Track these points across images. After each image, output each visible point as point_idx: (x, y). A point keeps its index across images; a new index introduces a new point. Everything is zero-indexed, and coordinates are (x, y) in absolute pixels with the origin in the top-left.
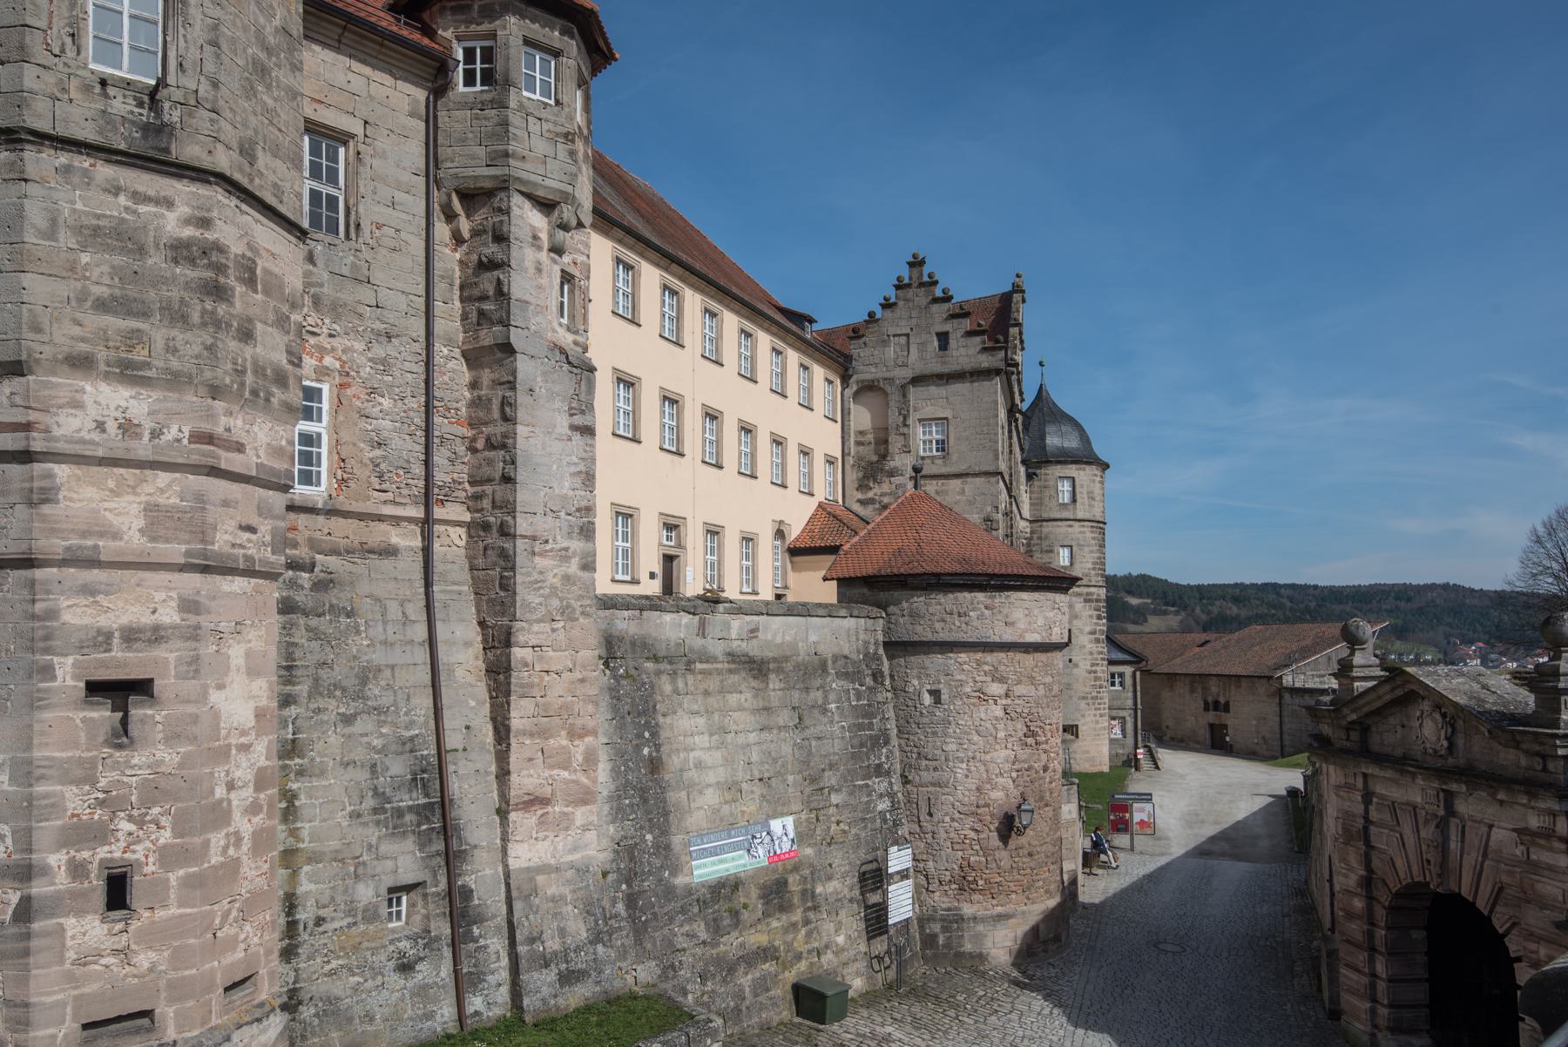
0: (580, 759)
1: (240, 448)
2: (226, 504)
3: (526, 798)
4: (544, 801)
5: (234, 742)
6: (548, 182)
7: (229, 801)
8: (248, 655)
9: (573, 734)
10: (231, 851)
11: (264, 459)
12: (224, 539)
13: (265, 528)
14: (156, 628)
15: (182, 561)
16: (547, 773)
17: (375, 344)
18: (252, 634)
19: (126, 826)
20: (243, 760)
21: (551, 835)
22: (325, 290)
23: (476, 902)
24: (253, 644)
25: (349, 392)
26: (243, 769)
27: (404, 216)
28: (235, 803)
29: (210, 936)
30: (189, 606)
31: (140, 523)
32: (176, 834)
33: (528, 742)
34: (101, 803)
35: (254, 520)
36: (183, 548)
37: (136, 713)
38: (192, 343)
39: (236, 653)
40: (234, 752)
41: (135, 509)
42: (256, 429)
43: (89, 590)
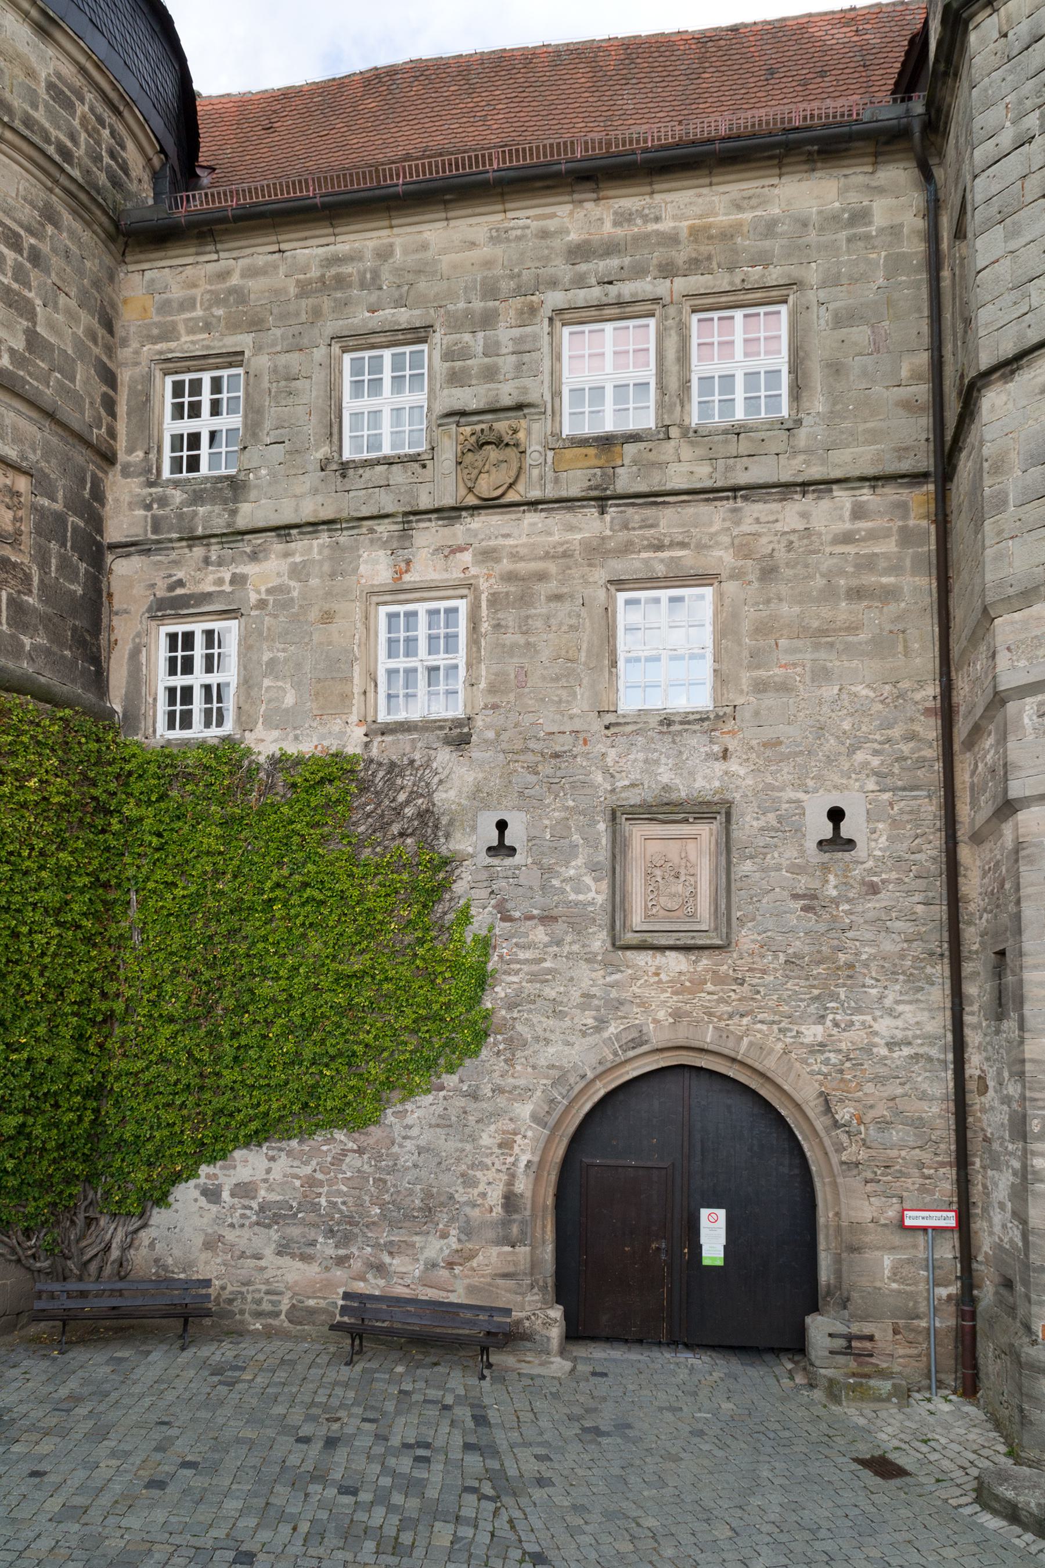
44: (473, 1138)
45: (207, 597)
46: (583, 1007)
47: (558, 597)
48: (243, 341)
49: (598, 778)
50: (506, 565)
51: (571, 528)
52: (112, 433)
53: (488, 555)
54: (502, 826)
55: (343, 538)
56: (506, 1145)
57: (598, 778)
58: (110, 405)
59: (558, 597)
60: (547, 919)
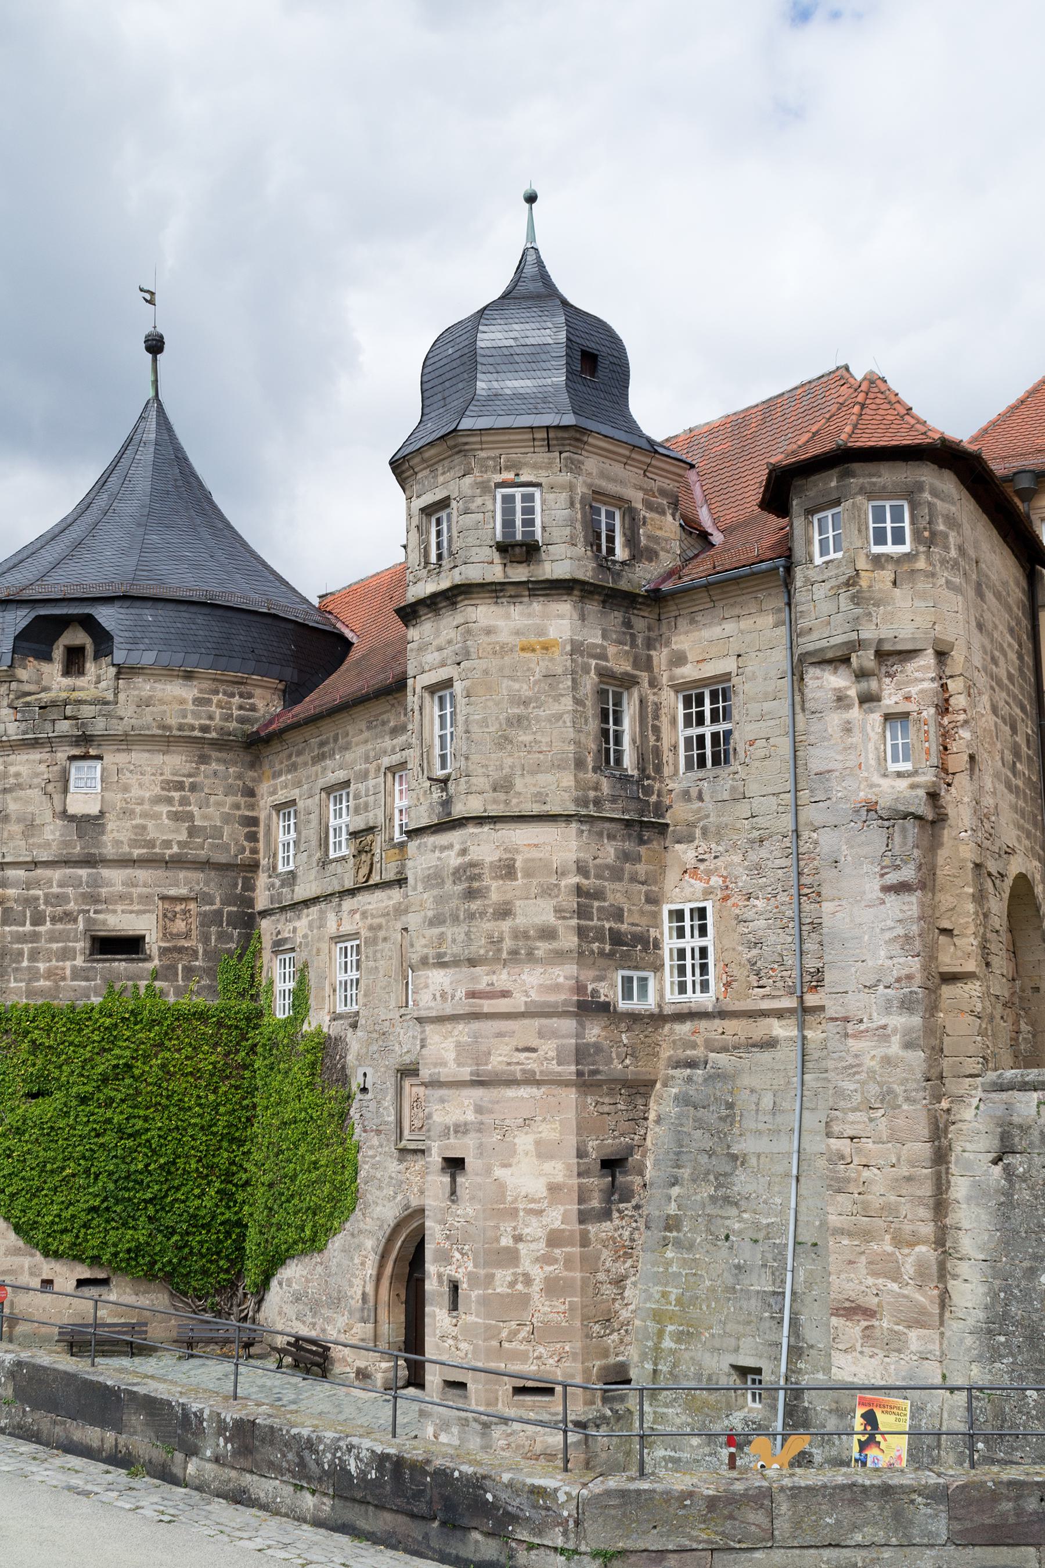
0: (911, 1271)
1: (505, 994)
2: (500, 1035)
3: (847, 1304)
4: (869, 1313)
5: (521, 1206)
6: (833, 641)
7: (517, 1251)
8: (538, 1143)
9: (898, 1241)
10: (519, 1287)
11: (534, 996)
12: (498, 1061)
13: (548, 1048)
14: (466, 1124)
15: (468, 1078)
16: (870, 1281)
17: (750, 852)
18: (544, 1127)
19: (458, 1255)
20: (534, 1220)
21: (881, 1355)
22: (711, 819)
23: (806, 1404)
24: (543, 1135)
25: (730, 903)
26: (534, 1228)
27: (772, 723)
28: (523, 1252)
29: (495, 1343)
30: (479, 1110)
31: (453, 1055)
32: (475, 1266)
33: (846, 1242)
34: (448, 1237)
35: (534, 1043)
36: (469, 1069)
37: (460, 1180)
38: (455, 932)
39: (524, 1141)
40: (521, 1214)
41: (452, 1045)
42: (523, 977)
43: (442, 1100)
44: (352, 1259)
45: (285, 940)
46: (389, 1185)
47: (385, 939)
48: (295, 793)
49: (397, 1048)
50: (369, 921)
51: (390, 898)
52: (255, 851)
53: (364, 915)
54: (365, 1075)
55: (323, 905)
56: (363, 1264)
57: (397, 1048)
58: (253, 837)
59: (385, 939)
60: (378, 1132)
